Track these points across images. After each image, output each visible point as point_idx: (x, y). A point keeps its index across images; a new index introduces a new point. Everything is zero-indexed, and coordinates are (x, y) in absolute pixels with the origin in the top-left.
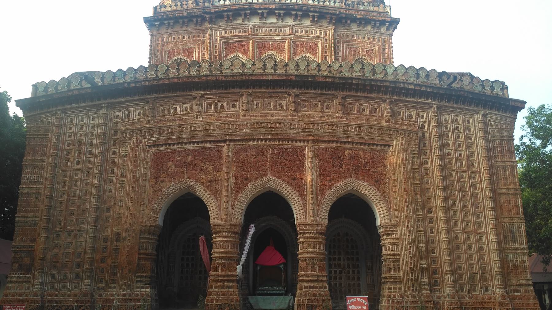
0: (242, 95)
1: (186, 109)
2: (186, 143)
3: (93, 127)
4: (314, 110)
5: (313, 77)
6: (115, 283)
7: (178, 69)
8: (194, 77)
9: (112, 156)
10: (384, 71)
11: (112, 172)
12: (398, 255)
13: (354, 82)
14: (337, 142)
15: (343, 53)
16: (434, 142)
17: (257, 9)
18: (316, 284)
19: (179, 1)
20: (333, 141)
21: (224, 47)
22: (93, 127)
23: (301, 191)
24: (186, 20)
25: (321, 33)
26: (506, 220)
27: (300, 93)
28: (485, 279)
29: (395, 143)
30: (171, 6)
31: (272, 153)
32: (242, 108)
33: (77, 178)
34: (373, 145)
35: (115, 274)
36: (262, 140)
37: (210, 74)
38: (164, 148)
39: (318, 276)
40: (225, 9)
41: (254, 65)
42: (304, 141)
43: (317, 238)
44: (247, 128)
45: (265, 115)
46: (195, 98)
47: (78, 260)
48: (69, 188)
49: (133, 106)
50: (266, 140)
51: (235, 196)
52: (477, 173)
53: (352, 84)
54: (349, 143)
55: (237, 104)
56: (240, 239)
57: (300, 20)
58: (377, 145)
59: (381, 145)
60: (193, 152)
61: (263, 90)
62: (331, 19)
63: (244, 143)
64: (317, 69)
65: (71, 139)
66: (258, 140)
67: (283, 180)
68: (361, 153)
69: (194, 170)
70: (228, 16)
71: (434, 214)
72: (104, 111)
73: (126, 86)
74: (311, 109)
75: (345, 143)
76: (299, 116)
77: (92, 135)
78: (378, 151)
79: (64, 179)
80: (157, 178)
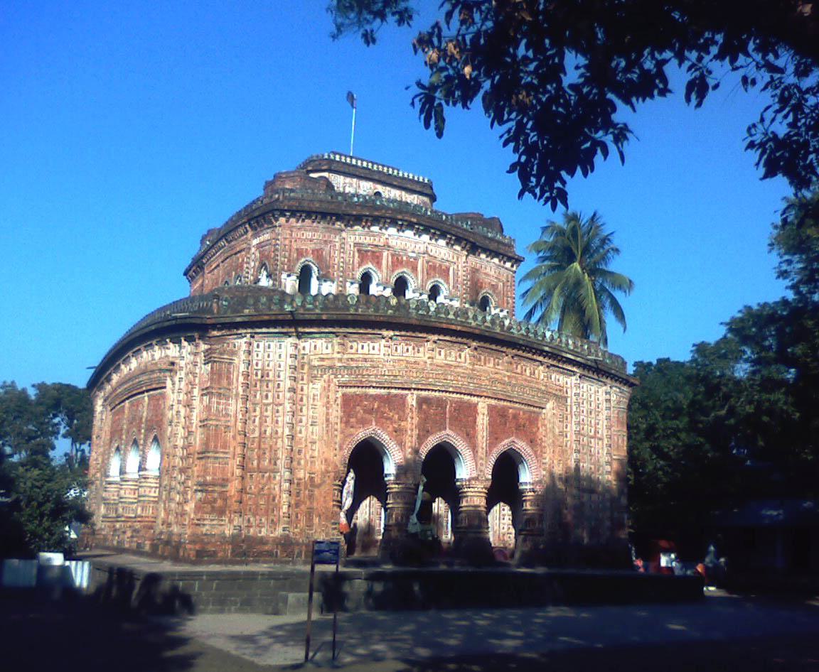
0: (428, 341)
1: (373, 349)
2: (374, 387)
3: (280, 356)
11: (301, 411)
14: (504, 400)
19: (310, 188)
20: (501, 399)
21: (357, 255)
22: (280, 356)
24: (319, 216)
25: (453, 258)
31: (451, 406)
32: (427, 355)
36: (443, 391)
42: (478, 396)
48: (261, 424)
49: (320, 338)
50: (446, 392)
52: (600, 439)
55: (421, 349)
57: (436, 240)
58: (534, 407)
61: (447, 338)
62: (466, 245)
63: (427, 393)
65: (260, 367)
66: (439, 391)
68: (521, 413)
69: (382, 417)
72: (293, 340)
74: (485, 364)
77: (280, 366)
79: (254, 414)
80: (347, 423)
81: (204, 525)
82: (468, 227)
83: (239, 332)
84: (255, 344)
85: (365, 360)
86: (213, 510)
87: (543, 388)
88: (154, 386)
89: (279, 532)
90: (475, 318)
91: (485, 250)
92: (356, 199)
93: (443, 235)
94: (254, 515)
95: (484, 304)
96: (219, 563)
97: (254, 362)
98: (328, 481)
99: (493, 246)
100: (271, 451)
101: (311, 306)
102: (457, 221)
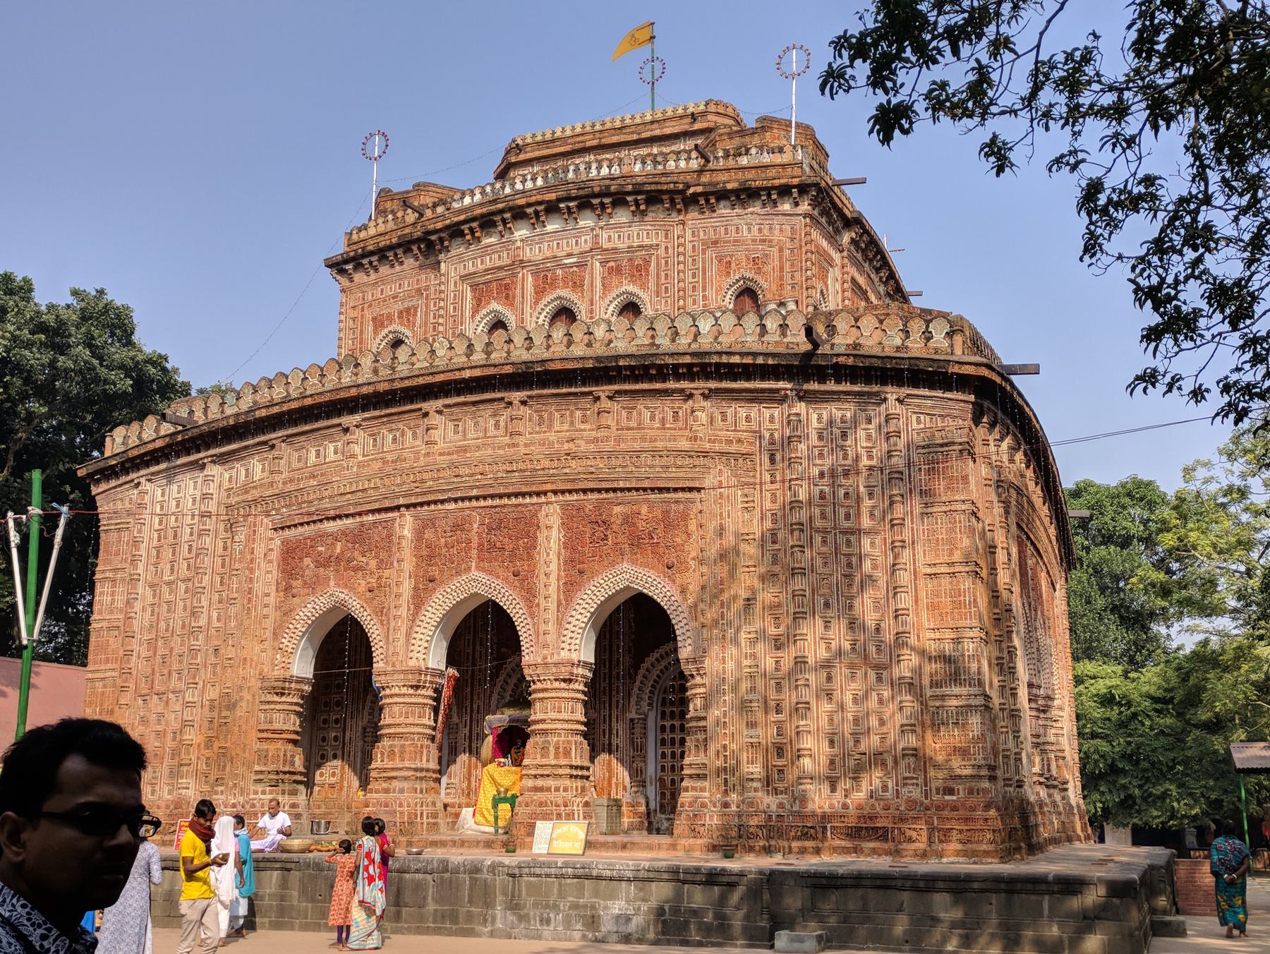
0: (426, 415)
1: (336, 453)
2: (334, 518)
4: (557, 428)
5: (543, 361)
6: (222, 785)
7: (323, 376)
9: (220, 551)
10: (694, 329)
12: (704, 718)
13: (621, 363)
14: (599, 490)
15: (704, 273)
19: (392, 212)
20: (592, 490)
23: (530, 595)
24: (400, 251)
27: (529, 397)
33: (172, 598)
34: (668, 490)
35: (224, 769)
36: (463, 499)
37: (375, 379)
40: (462, 218)
41: (451, 348)
42: (538, 494)
44: (433, 479)
45: (464, 449)
46: (346, 430)
50: (470, 499)
51: (413, 615)
53: (619, 368)
54: (622, 490)
56: (435, 699)
58: (676, 490)
59: (683, 489)
60: (344, 533)
61: (461, 399)
62: (672, 201)
64: (566, 339)
66: (456, 500)
67: (498, 577)
68: (644, 510)
73: (231, 422)
74: (550, 426)
75: (614, 490)
76: (526, 445)
78: (677, 502)
80: (288, 588)
83: (129, 478)
84: (160, 492)
91: (723, 195)
92: (467, 200)
93: (619, 200)
98: (250, 697)
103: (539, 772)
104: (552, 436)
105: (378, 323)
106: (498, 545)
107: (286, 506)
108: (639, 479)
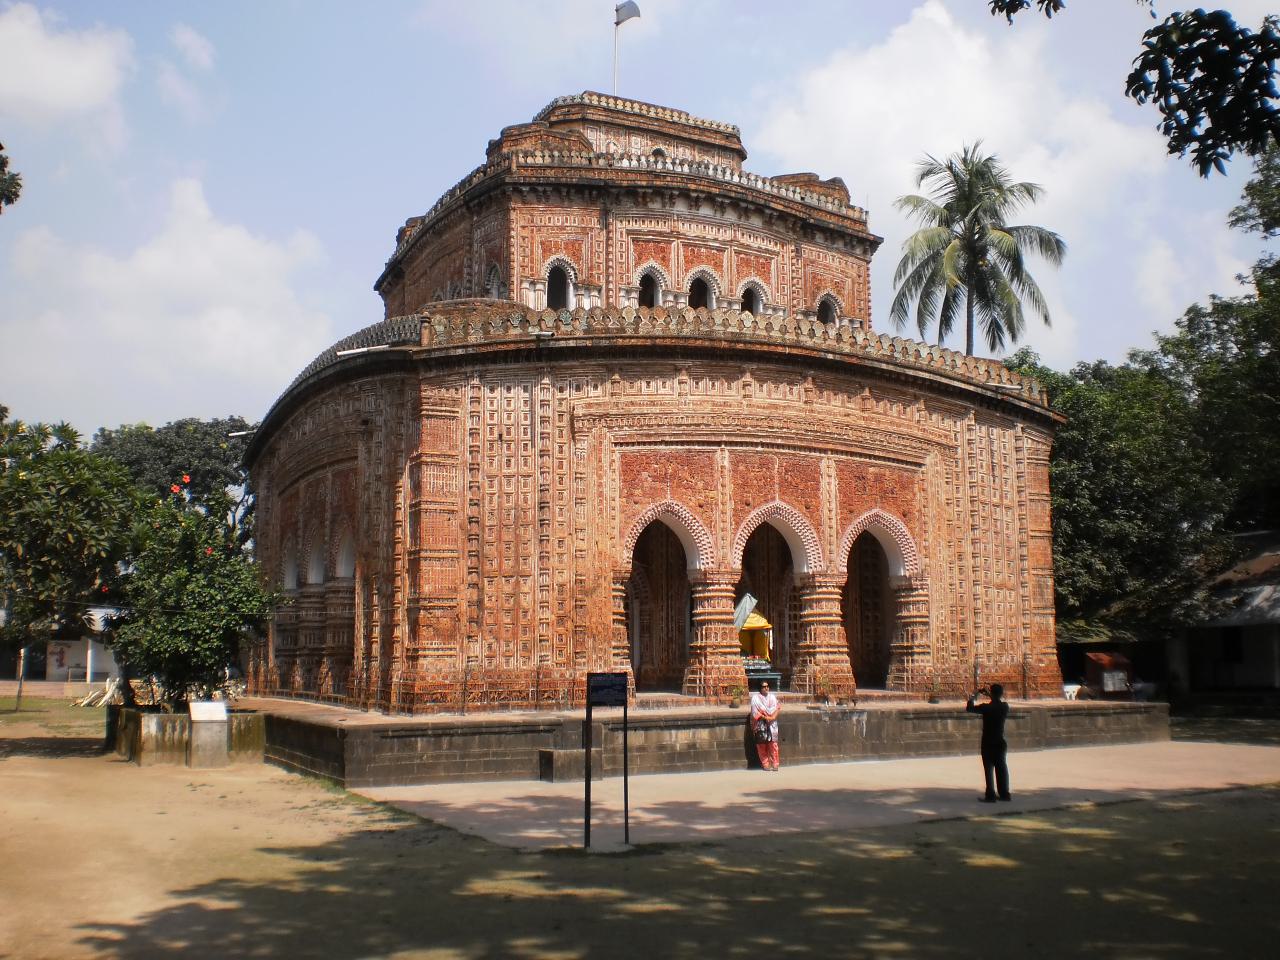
0: (743, 372)
4: (833, 403)
8: (686, 338)
12: (927, 617)
14: (861, 455)
16: (968, 462)
17: (689, 190)
18: (837, 657)
19: (556, 148)
21: (632, 247)
23: (818, 525)
26: (1035, 572)
28: (1012, 648)
29: (928, 460)
30: (543, 157)
32: (743, 392)
33: (511, 489)
35: (583, 643)
38: (636, 448)
39: (839, 646)
40: (644, 183)
42: (821, 450)
43: (836, 593)
45: (776, 407)
47: (523, 621)
48: (500, 504)
52: (1008, 508)
57: (748, 218)
58: (907, 463)
62: (795, 223)
66: (763, 445)
68: (887, 473)
70: (644, 193)
71: (964, 562)
74: (829, 401)
75: (870, 456)
76: (819, 413)
80: (630, 495)
81: (425, 656)
82: (798, 198)
83: (463, 370)
85: (653, 403)
86: (438, 633)
87: (920, 434)
88: (340, 456)
89: (534, 663)
90: (812, 333)
92: (625, 163)
93: (760, 210)
94: (497, 640)
95: (825, 313)
96: (448, 710)
97: (488, 415)
99: (832, 222)
100: (517, 547)
101: (569, 328)
102: (779, 188)
103: (830, 650)
104: (837, 410)
105: (547, 250)
106: (794, 484)
107: (630, 426)
108: (888, 452)
